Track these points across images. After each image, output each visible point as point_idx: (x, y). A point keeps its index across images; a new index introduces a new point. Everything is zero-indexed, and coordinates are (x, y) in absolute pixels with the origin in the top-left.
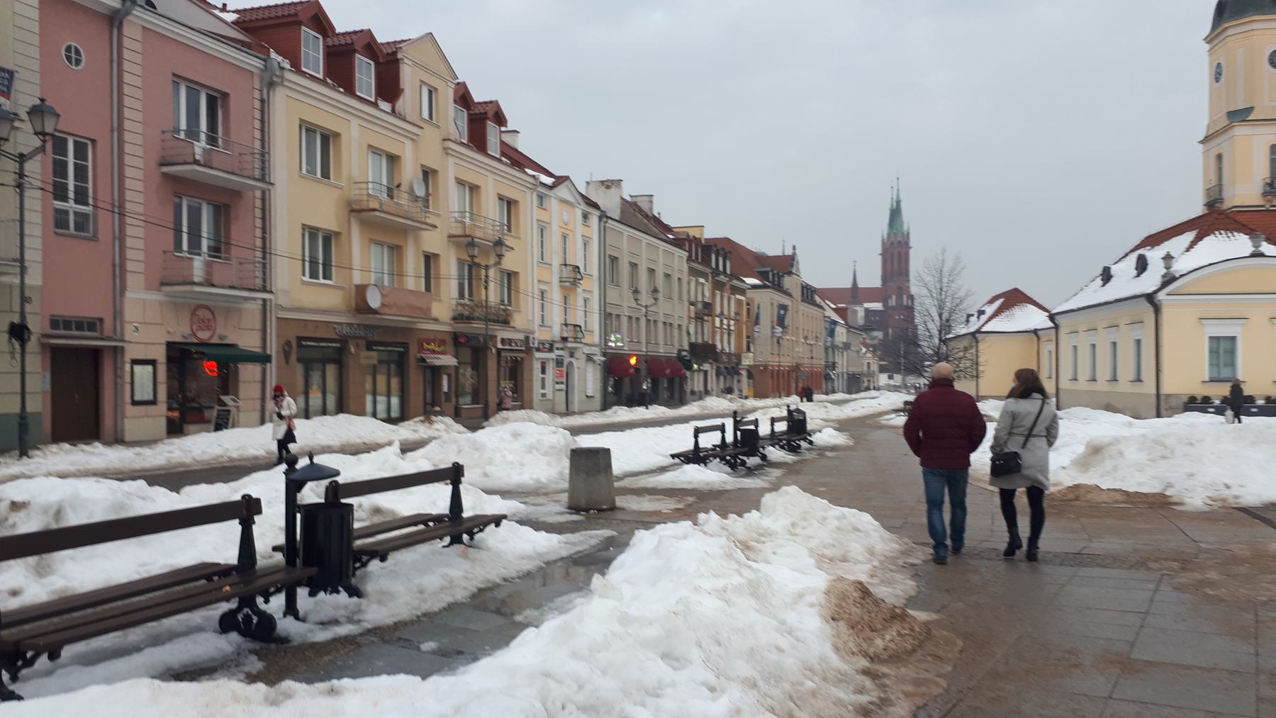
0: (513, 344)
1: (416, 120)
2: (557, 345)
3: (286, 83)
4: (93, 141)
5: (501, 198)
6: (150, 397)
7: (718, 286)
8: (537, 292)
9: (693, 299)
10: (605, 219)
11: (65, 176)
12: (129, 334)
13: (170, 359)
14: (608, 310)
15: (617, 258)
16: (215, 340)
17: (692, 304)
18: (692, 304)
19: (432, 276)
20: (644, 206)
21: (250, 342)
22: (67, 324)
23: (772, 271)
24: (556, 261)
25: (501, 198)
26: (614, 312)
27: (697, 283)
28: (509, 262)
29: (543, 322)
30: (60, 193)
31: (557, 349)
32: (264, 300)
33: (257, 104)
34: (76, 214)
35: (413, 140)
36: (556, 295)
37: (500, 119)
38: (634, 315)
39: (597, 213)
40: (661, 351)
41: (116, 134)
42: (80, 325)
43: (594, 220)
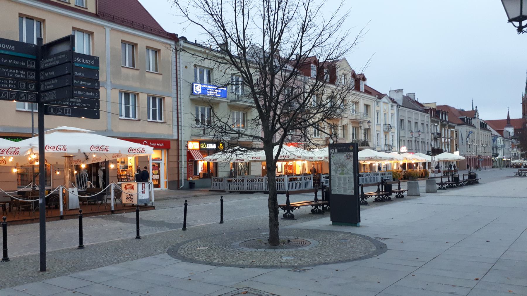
6: (281, 171)
7: (443, 126)
9: (432, 132)
14: (400, 139)
15: (403, 120)
17: (432, 134)
18: (432, 134)
20: (412, 97)
23: (466, 117)
24: (382, 123)
25: (365, 105)
26: (403, 139)
27: (434, 125)
36: (382, 135)
37: (364, 79)
39: (396, 105)
43: (395, 107)
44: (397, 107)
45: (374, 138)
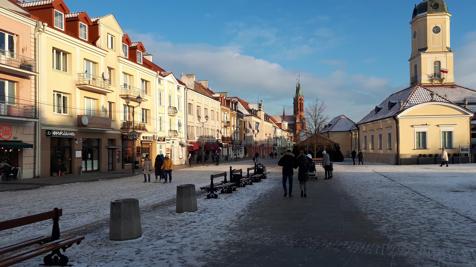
0: (148, 139)
2: (166, 139)
3: (46, 31)
5: (143, 80)
8: (158, 118)
10: (187, 89)
16: (12, 139)
17: (222, 122)
19: (112, 111)
21: (28, 139)
24: (167, 105)
25: (143, 80)
29: (161, 129)
31: (167, 140)
32: (36, 122)
35: (104, 56)
37: (142, 49)
40: (210, 140)
44: (185, 90)
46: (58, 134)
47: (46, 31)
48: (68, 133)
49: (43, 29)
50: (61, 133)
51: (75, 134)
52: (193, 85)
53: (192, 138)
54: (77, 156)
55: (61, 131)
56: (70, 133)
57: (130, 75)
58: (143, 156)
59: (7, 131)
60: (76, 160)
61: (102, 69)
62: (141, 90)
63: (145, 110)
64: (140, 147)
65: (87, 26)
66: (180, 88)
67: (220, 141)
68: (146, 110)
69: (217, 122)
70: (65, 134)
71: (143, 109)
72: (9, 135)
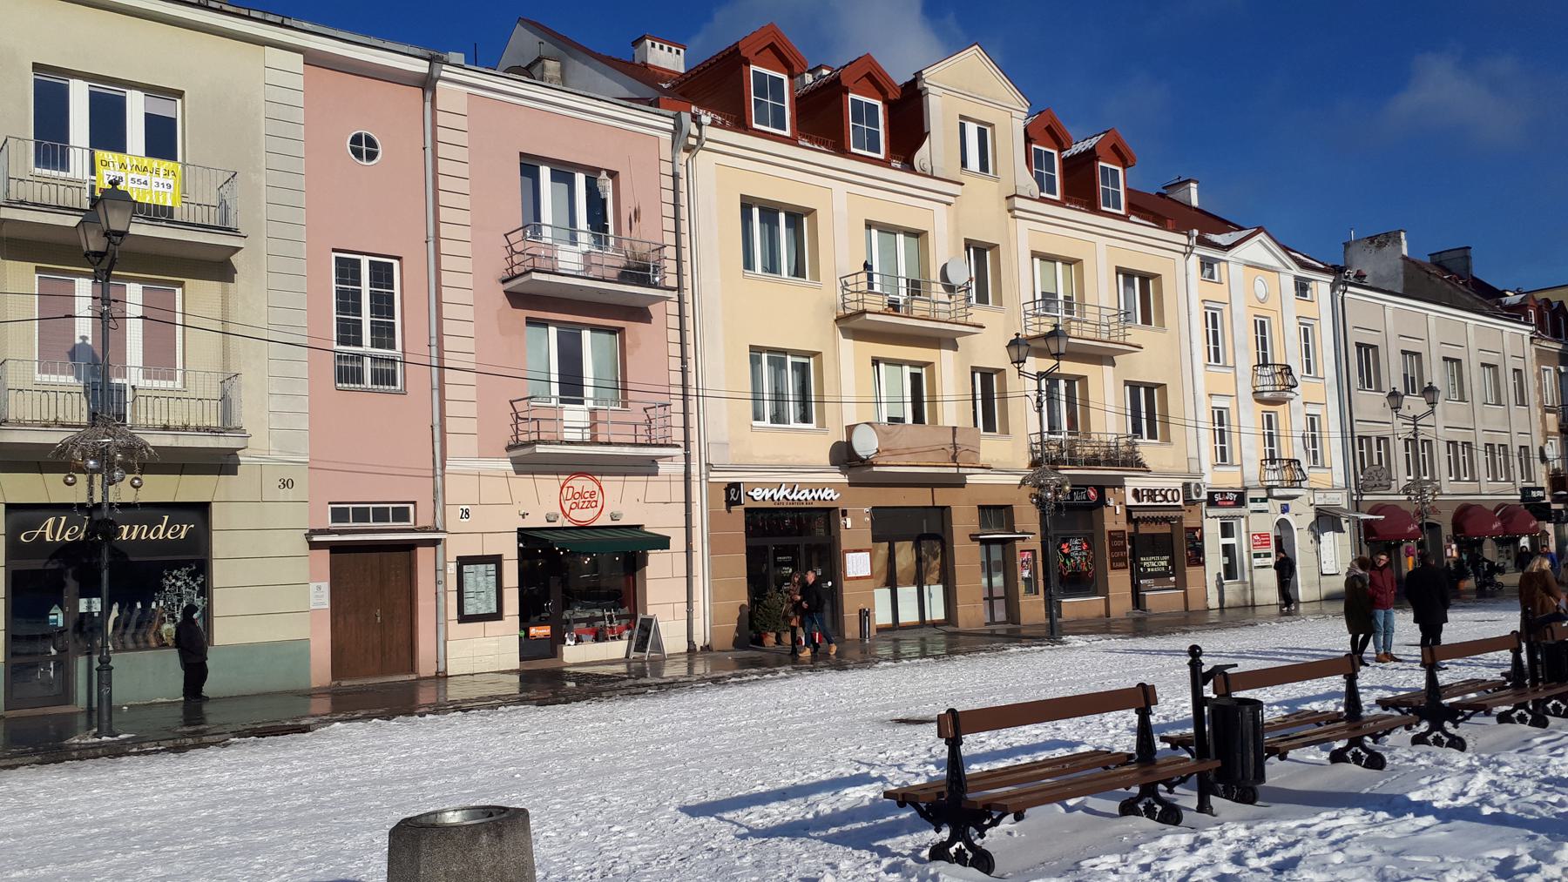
0: (1159, 498)
1: (955, 172)
2: (1250, 494)
3: (707, 145)
4: (399, 258)
5: (1128, 275)
8: (1205, 416)
11: (357, 310)
12: (453, 521)
13: (523, 555)
14: (1360, 430)
16: (604, 520)
21: (660, 517)
22: (361, 515)
28: (1143, 368)
30: (349, 333)
31: (1254, 500)
33: (668, 182)
34: (375, 359)
35: (949, 204)
38: (1460, 437)
41: (431, 244)
42: (381, 515)
44: (1333, 291)
45: (1191, 432)
46: (773, 495)
47: (707, 145)
48: (811, 491)
49: (699, 138)
50: (782, 493)
51: (838, 495)
52: (1398, 274)
53: (1381, 485)
54: (850, 574)
55: (784, 485)
56: (820, 491)
57: (1068, 262)
58: (1146, 568)
59: (587, 495)
60: (845, 584)
61: (945, 251)
62: (1116, 312)
63: (1142, 390)
64: (1124, 531)
65: (879, 104)
66: (1312, 285)
67: (1540, 493)
68: (1150, 388)
69: (1518, 413)
70: (799, 496)
71: (1134, 387)
72: (596, 506)
